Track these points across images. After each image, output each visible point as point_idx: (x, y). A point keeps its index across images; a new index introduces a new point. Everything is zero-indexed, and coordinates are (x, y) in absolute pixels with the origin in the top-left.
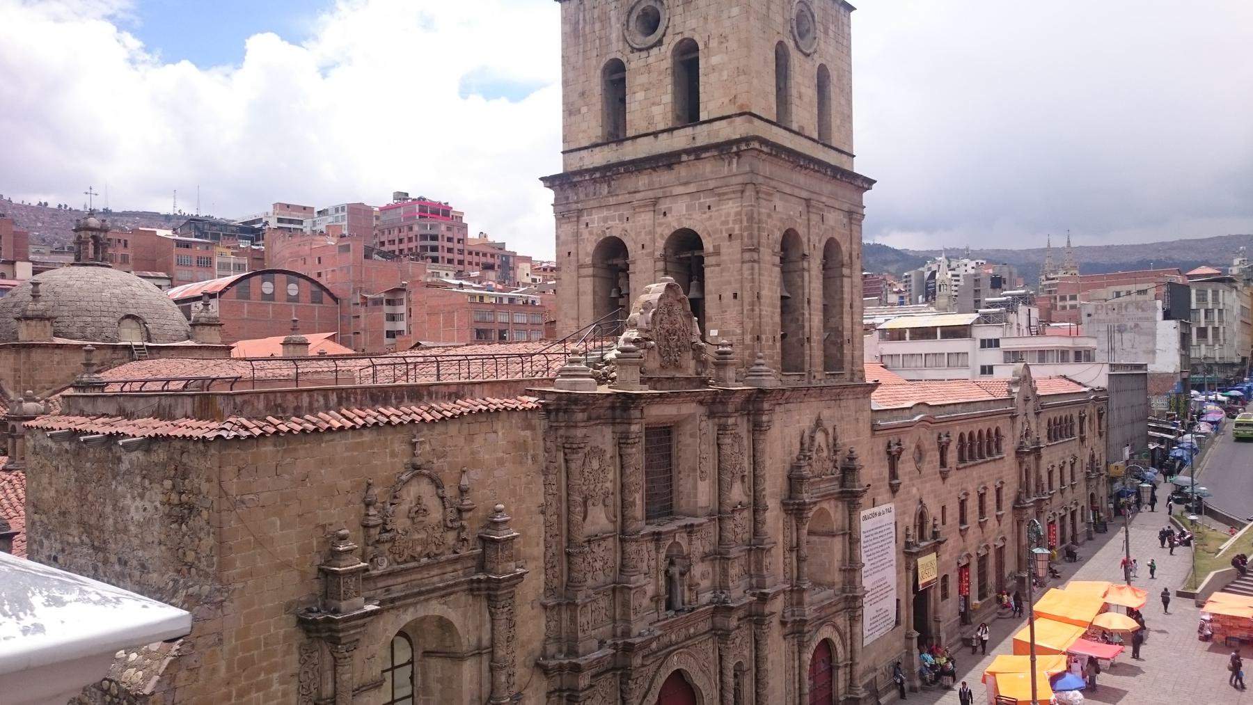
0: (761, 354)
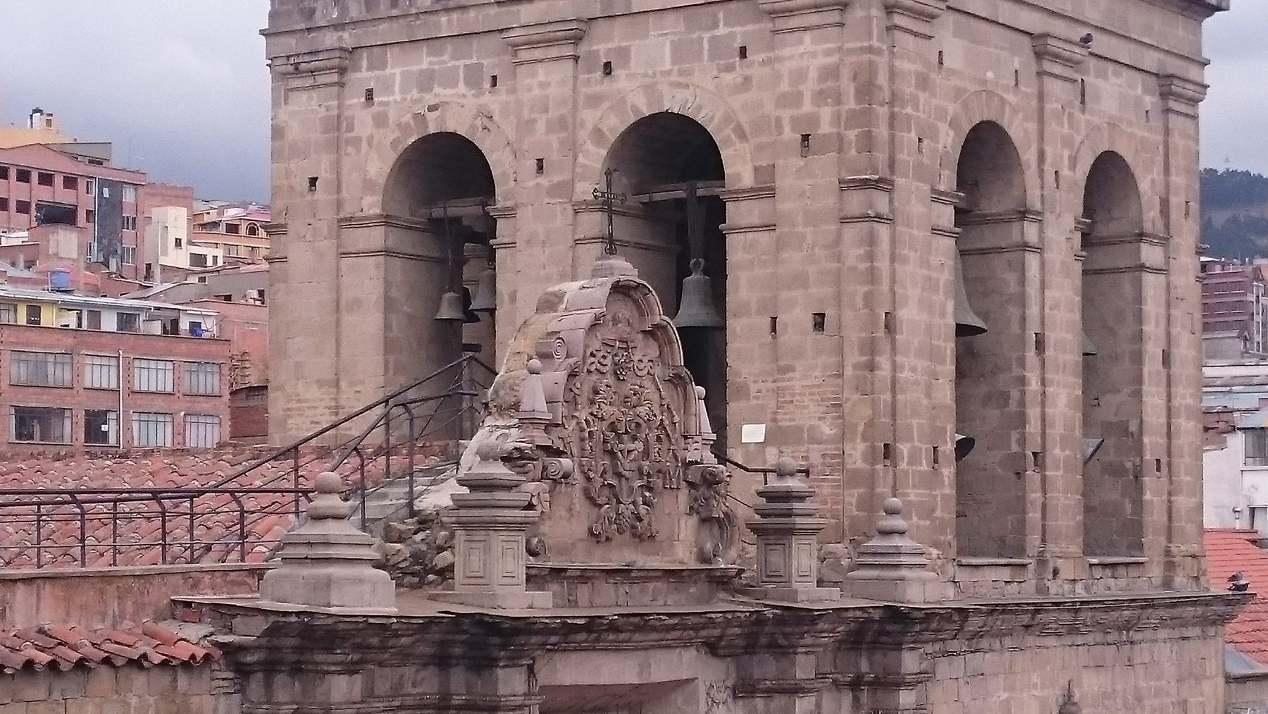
0: (895, 502)
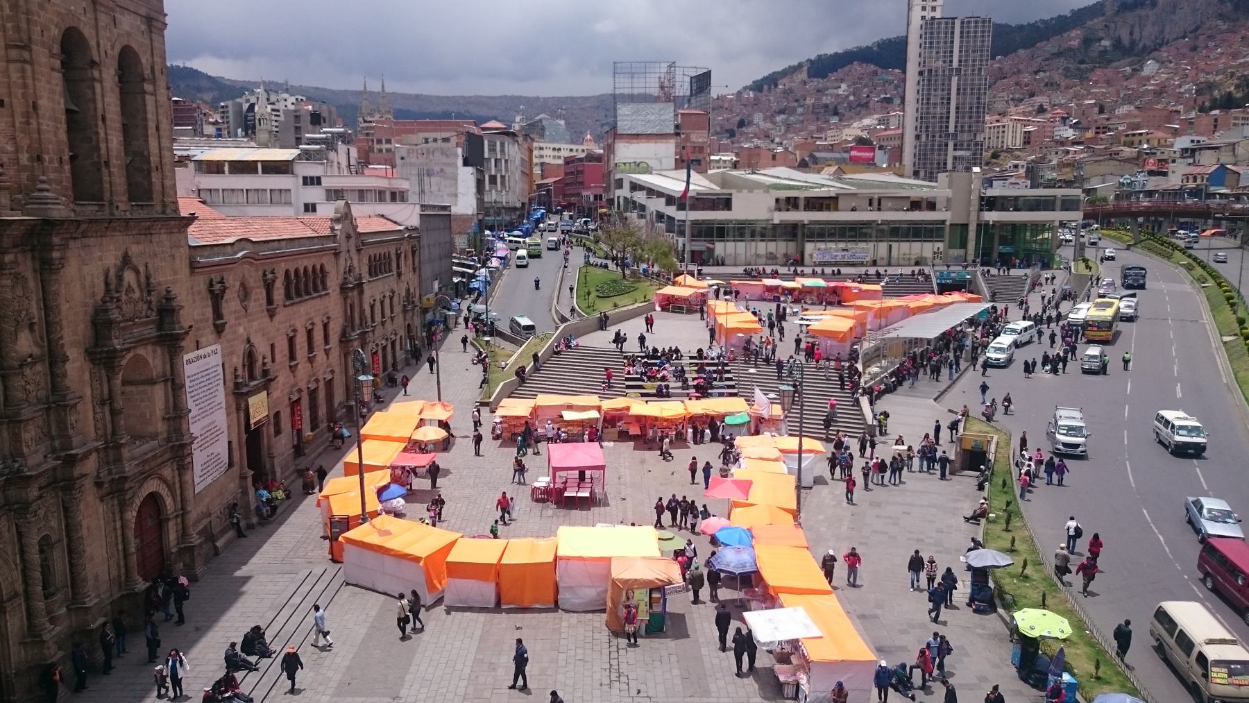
0: (45, 178)
